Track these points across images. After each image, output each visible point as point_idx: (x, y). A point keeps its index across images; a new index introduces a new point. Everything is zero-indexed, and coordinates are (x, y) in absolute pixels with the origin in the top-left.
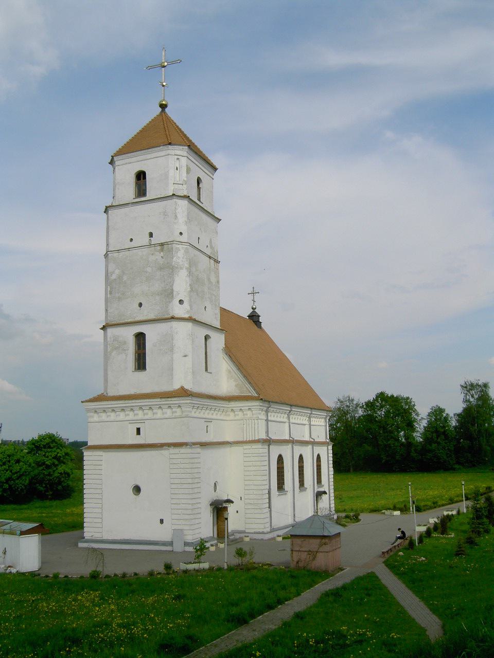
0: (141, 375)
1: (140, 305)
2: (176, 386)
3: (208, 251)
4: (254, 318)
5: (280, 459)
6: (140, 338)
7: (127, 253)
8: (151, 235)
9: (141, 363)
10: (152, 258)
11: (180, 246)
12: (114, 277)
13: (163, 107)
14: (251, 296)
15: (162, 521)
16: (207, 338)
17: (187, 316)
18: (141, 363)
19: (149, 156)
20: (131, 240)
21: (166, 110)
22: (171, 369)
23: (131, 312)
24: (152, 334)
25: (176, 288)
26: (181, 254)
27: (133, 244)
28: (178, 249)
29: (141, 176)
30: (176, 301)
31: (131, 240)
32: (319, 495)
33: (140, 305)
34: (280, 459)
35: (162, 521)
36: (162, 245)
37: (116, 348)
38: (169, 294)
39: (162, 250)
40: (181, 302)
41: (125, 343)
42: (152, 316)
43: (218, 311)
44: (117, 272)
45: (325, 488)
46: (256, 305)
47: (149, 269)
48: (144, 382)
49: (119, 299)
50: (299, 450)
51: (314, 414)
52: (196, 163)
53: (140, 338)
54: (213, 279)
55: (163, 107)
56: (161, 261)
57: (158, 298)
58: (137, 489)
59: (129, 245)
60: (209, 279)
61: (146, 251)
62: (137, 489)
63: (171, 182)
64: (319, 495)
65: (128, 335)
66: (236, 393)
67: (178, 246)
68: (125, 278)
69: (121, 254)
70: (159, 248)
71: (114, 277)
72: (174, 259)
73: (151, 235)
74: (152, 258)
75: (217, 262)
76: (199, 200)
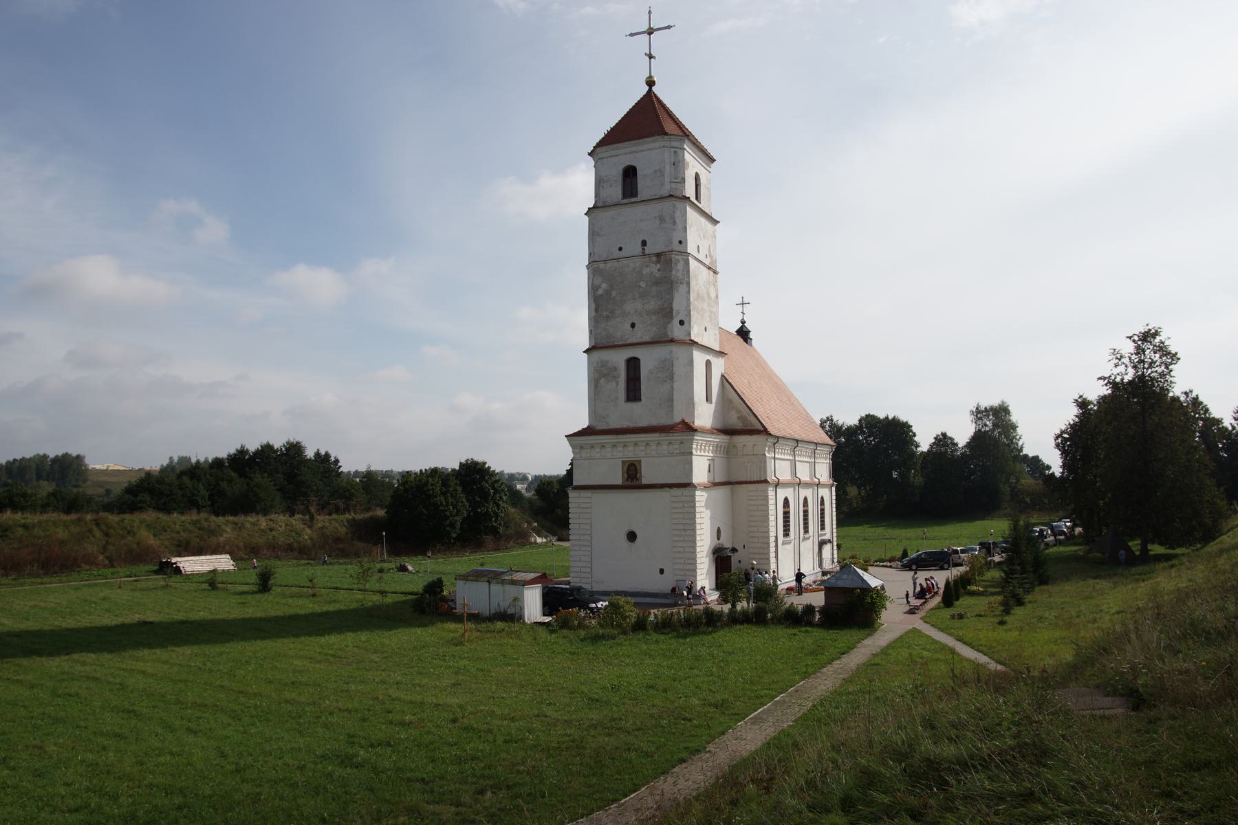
0: (634, 406)
1: (633, 325)
2: (677, 420)
3: (707, 262)
5: (786, 501)
6: (633, 365)
7: (615, 264)
8: (644, 243)
9: (633, 393)
10: (646, 271)
11: (680, 257)
12: (600, 292)
13: (650, 83)
14: (740, 308)
15: (662, 571)
16: (708, 364)
18: (633, 393)
19: (640, 148)
20: (620, 249)
21: (654, 89)
22: (671, 400)
23: (620, 329)
24: (649, 359)
26: (680, 266)
27: (622, 254)
29: (630, 174)
30: (676, 322)
31: (620, 249)
32: (822, 544)
33: (633, 325)
34: (786, 501)
35: (662, 571)
36: (658, 255)
37: (605, 375)
38: (666, 313)
39: (658, 262)
40: (682, 323)
41: (616, 369)
42: (647, 339)
43: (717, 332)
44: (604, 286)
45: (828, 537)
47: (643, 284)
48: (640, 414)
49: (608, 318)
50: (804, 492)
53: (633, 365)
54: (713, 295)
55: (650, 83)
56: (658, 274)
57: (654, 317)
58: (632, 536)
59: (617, 254)
60: (708, 294)
61: (638, 262)
62: (632, 536)
63: (667, 180)
64: (822, 544)
65: (619, 359)
68: (614, 294)
69: (610, 264)
70: (654, 259)
71: (600, 292)
73: (644, 243)
74: (646, 271)
75: (715, 272)
76: (697, 198)
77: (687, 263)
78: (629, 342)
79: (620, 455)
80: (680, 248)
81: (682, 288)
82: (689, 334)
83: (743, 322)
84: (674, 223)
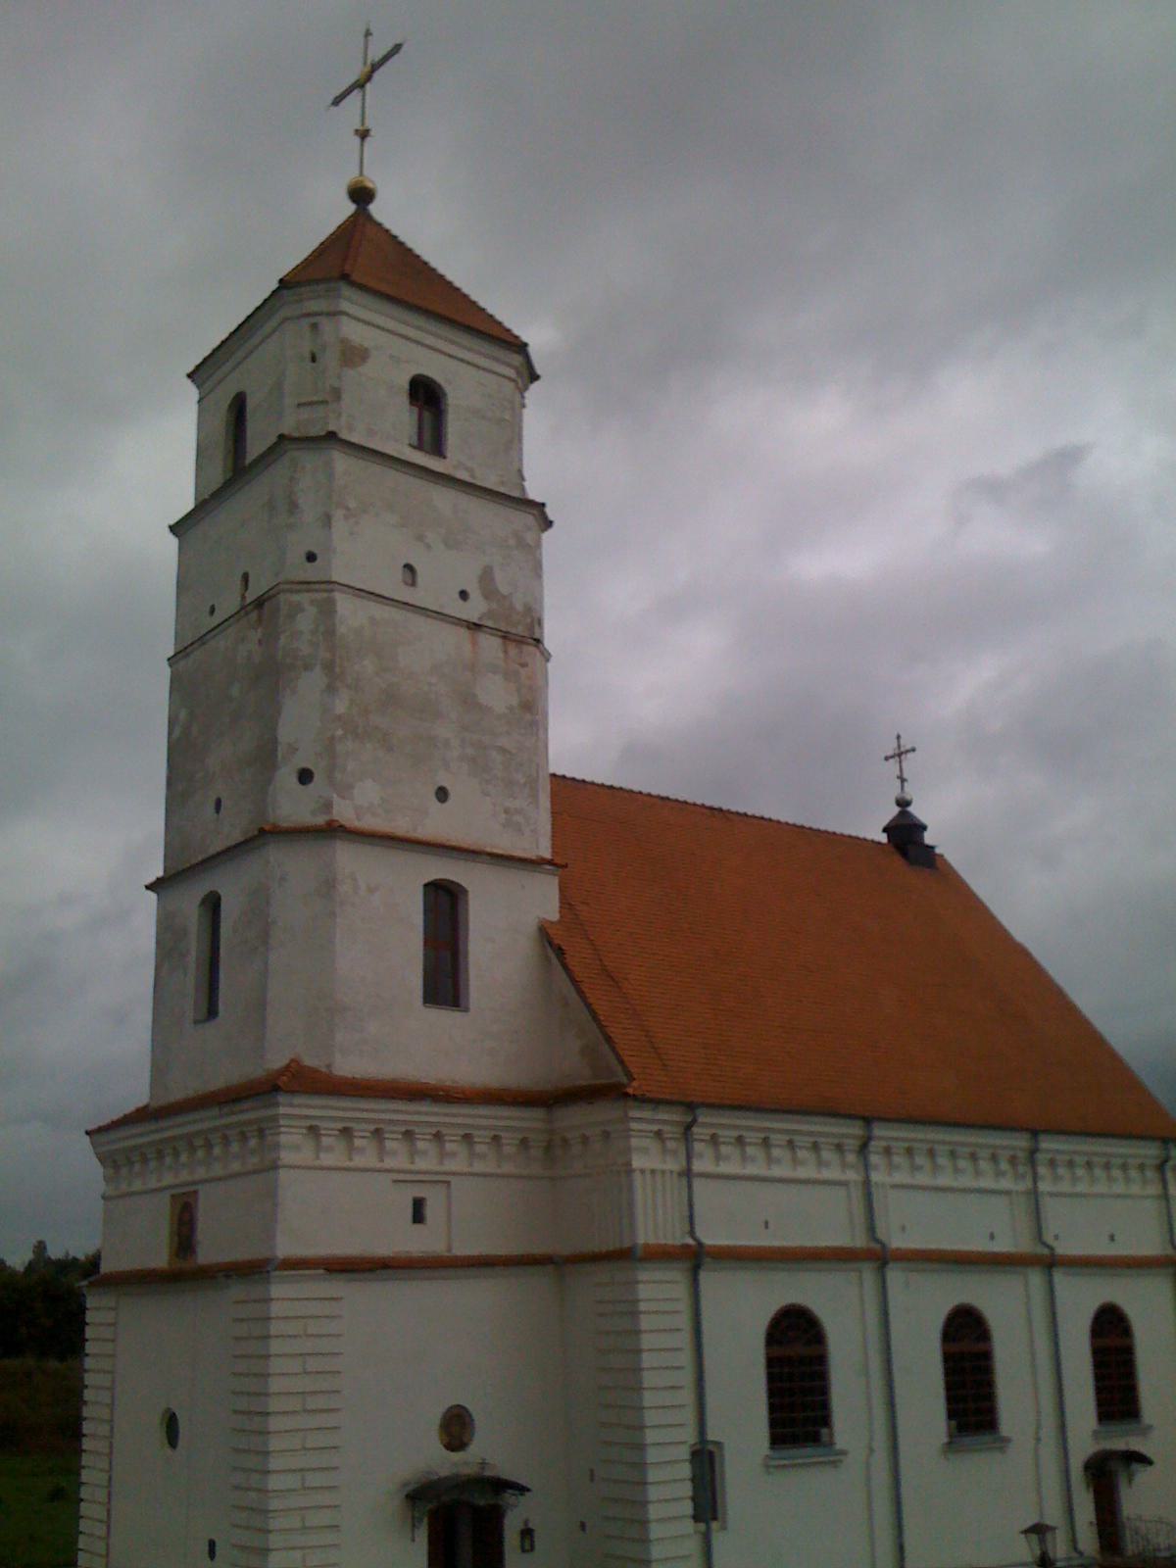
2: (277, 1061)
4: (905, 833)
11: (303, 598)
13: (361, 195)
14: (893, 766)
17: (320, 820)
20: (212, 610)
25: (285, 733)
26: (305, 622)
28: (298, 608)
30: (286, 777)
31: (212, 610)
40: (305, 776)
46: (910, 792)
51: (881, 1138)
52: (412, 333)
55: (361, 195)
66: (584, 1078)
67: (296, 598)
72: (283, 640)
77: (328, 610)
78: (212, 851)
79: (168, 1179)
80: (310, 572)
81: (311, 683)
82: (328, 806)
83: (903, 803)
84: (293, 507)
